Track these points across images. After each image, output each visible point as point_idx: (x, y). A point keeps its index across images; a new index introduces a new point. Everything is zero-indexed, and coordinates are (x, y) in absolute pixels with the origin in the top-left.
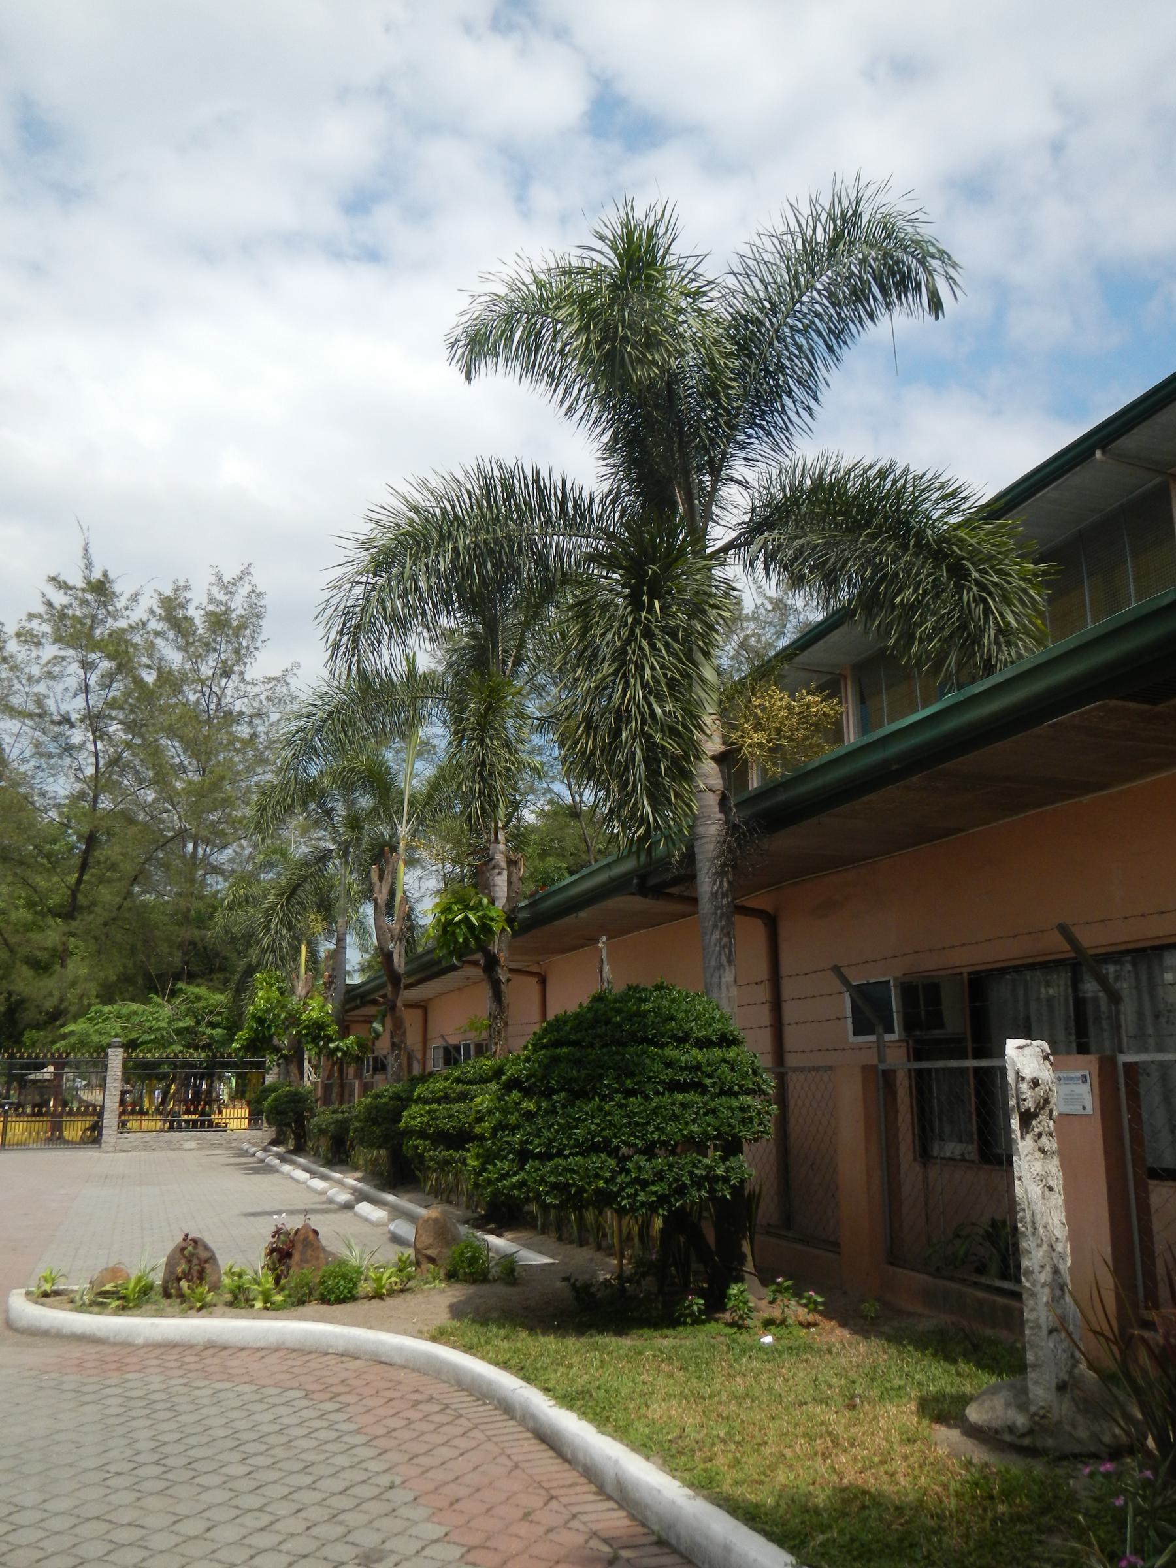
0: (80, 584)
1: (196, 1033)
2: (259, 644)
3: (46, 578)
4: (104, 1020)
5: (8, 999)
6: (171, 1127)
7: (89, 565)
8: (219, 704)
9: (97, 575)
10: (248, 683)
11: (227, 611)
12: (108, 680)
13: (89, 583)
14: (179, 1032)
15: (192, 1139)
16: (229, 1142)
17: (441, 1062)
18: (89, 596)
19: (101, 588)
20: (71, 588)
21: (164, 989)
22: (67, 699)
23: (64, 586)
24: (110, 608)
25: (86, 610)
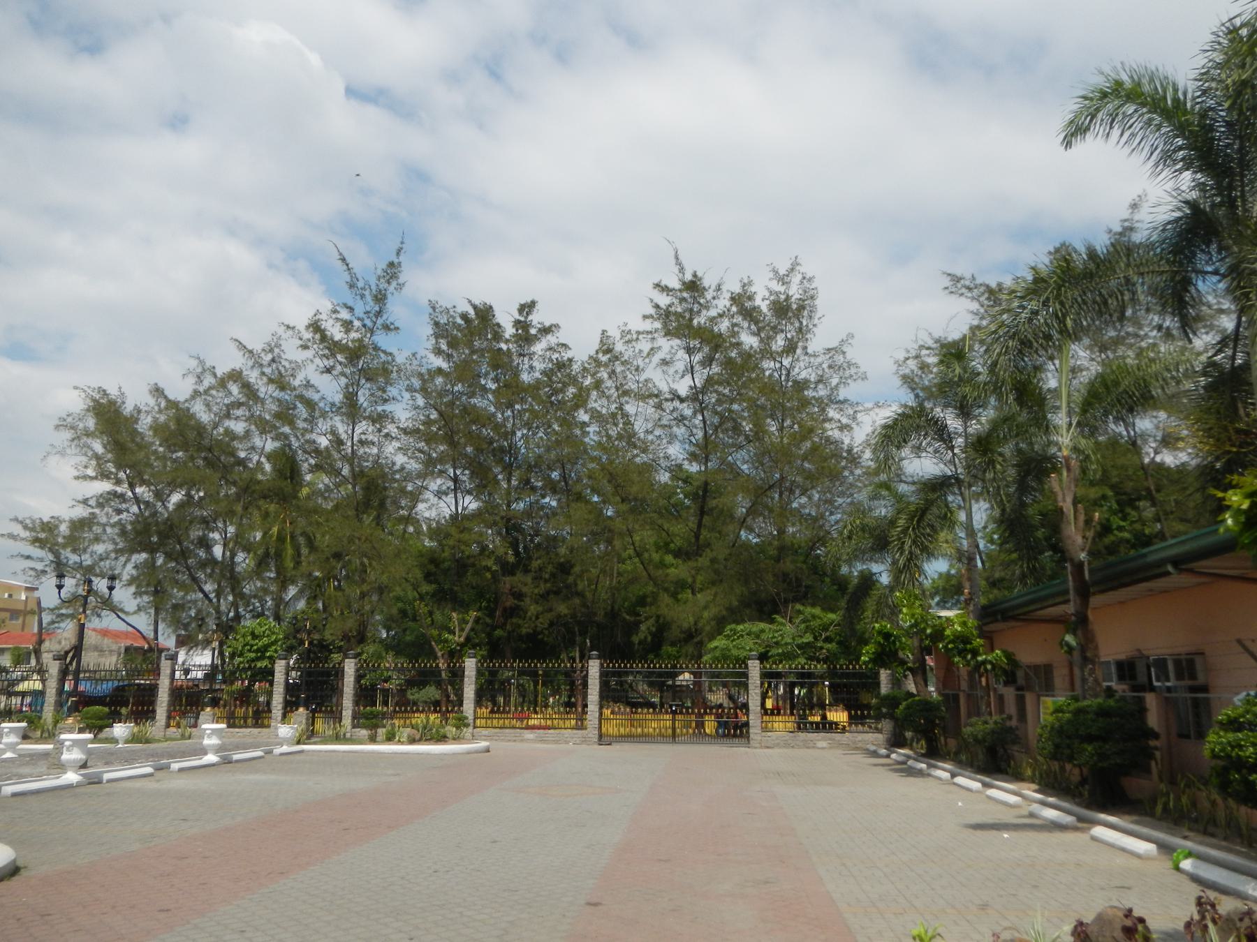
0: (677, 285)
1: (815, 647)
2: (816, 321)
3: (652, 286)
4: (738, 638)
5: (657, 621)
6: (799, 728)
7: (682, 270)
8: (788, 375)
9: (688, 277)
10: (811, 356)
11: (788, 298)
12: (707, 362)
13: (684, 283)
14: (799, 647)
15: (823, 739)
16: (854, 743)
17: (1115, 677)
18: (685, 295)
19: (693, 286)
20: (671, 291)
21: (786, 613)
22: (677, 379)
23: (665, 289)
24: (702, 301)
25: (685, 305)
